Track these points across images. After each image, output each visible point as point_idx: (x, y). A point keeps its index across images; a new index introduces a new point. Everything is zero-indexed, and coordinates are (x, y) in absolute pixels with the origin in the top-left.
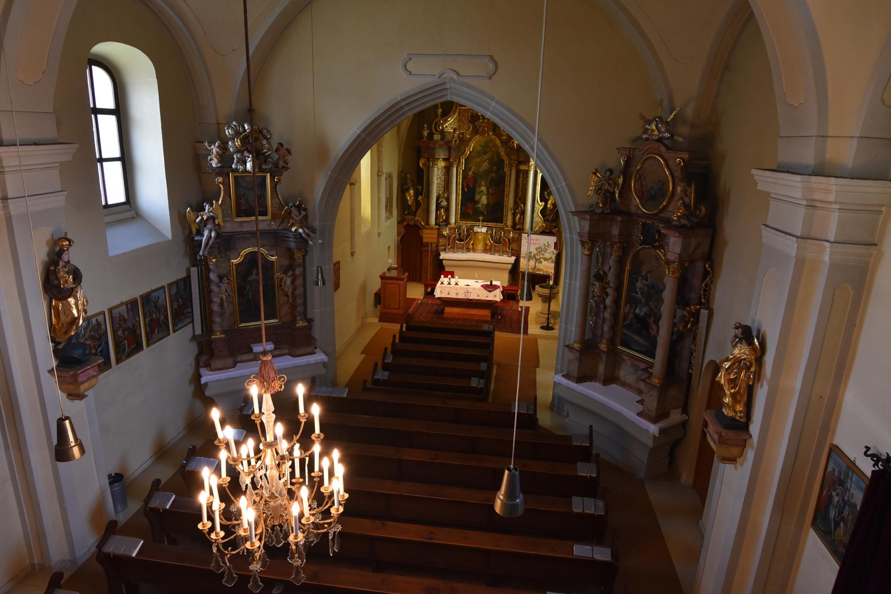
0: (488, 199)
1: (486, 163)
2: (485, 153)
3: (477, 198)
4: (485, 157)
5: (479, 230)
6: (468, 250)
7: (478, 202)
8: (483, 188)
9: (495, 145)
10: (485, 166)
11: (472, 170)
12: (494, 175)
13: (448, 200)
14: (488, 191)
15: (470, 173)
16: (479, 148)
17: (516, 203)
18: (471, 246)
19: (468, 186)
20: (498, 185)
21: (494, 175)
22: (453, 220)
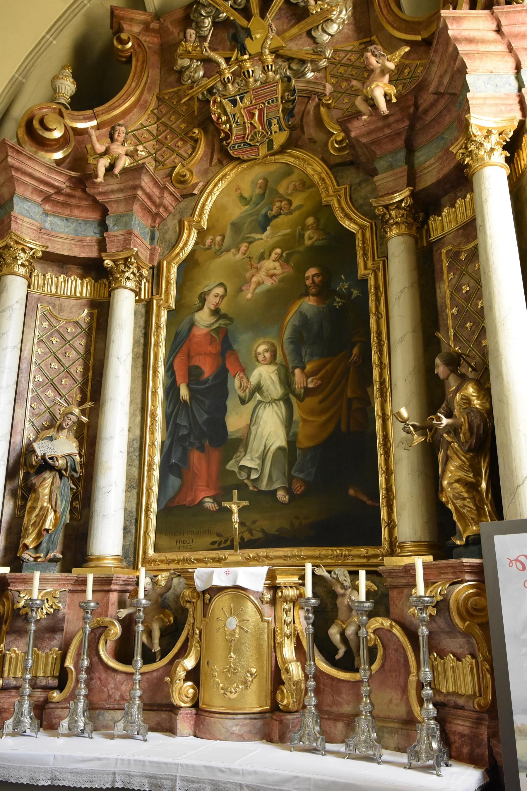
0: (289, 423)
1: (269, 264)
2: (264, 223)
3: (235, 421)
4: (266, 238)
5: (220, 577)
6: (161, 715)
7: (241, 443)
8: (265, 374)
9: (306, 184)
10: (269, 272)
11: (212, 301)
12: (309, 304)
13: (89, 437)
14: (286, 381)
15: (204, 318)
16: (237, 211)
17: (433, 396)
18: (182, 692)
19: (193, 375)
20: (336, 342)
21: (309, 304)
22: (108, 539)
